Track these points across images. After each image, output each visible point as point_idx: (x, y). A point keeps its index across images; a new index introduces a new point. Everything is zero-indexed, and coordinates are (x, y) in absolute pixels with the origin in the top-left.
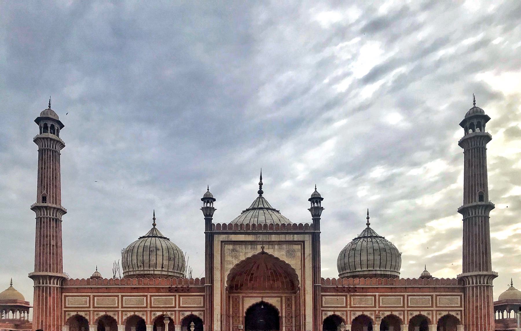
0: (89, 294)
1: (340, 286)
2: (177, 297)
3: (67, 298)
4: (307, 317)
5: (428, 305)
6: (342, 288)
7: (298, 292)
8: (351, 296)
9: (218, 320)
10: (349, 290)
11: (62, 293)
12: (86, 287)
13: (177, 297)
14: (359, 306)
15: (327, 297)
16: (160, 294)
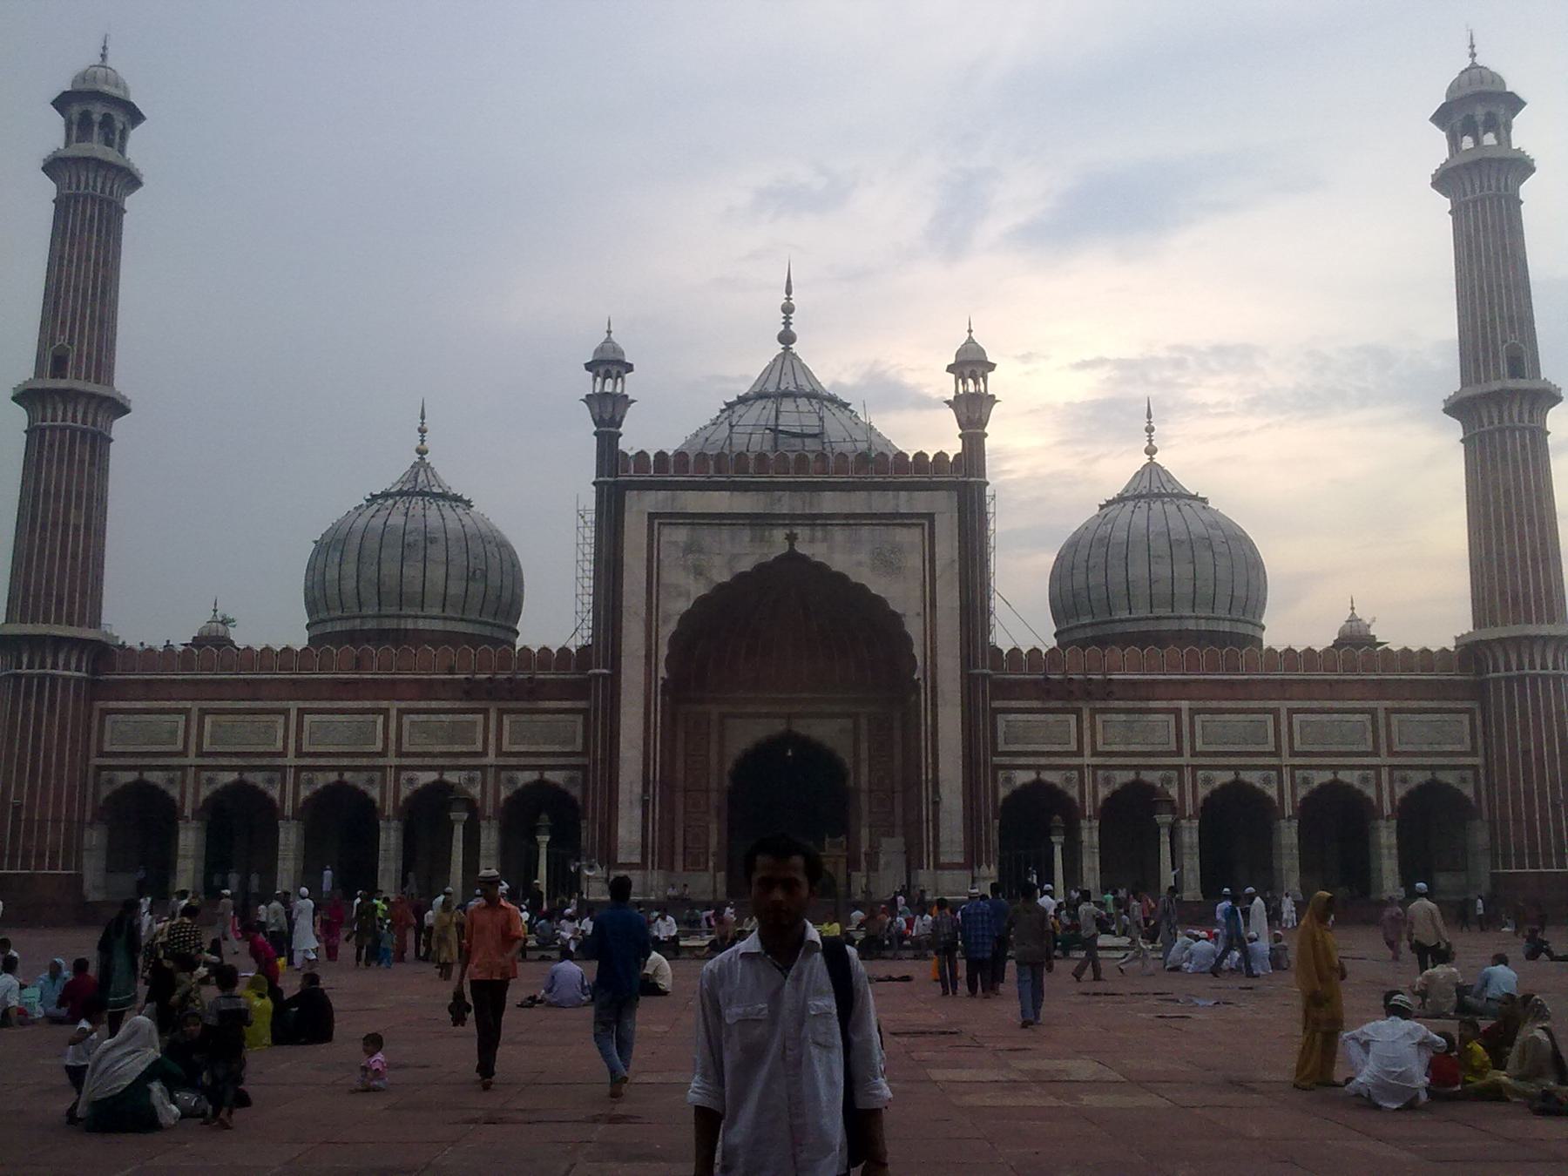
0: (188, 704)
1: (1056, 677)
2: (493, 716)
3: (109, 719)
4: (944, 791)
5: (1362, 748)
6: (1060, 682)
7: (913, 698)
8: (1094, 712)
9: (631, 803)
10: (1089, 691)
11: (93, 699)
12: (180, 677)
13: (493, 716)
14: (1122, 748)
15: (1012, 717)
16: (434, 704)
